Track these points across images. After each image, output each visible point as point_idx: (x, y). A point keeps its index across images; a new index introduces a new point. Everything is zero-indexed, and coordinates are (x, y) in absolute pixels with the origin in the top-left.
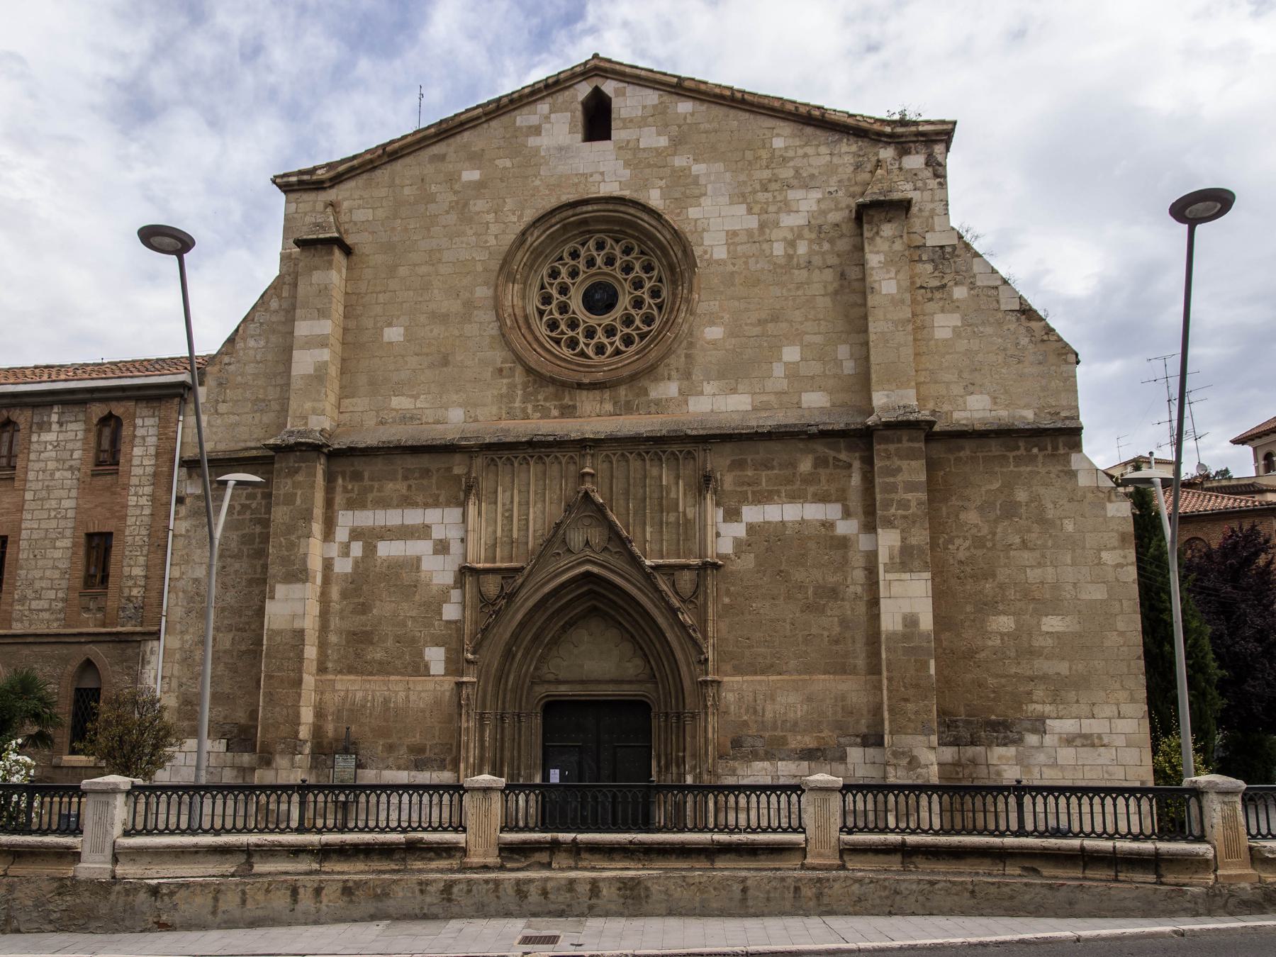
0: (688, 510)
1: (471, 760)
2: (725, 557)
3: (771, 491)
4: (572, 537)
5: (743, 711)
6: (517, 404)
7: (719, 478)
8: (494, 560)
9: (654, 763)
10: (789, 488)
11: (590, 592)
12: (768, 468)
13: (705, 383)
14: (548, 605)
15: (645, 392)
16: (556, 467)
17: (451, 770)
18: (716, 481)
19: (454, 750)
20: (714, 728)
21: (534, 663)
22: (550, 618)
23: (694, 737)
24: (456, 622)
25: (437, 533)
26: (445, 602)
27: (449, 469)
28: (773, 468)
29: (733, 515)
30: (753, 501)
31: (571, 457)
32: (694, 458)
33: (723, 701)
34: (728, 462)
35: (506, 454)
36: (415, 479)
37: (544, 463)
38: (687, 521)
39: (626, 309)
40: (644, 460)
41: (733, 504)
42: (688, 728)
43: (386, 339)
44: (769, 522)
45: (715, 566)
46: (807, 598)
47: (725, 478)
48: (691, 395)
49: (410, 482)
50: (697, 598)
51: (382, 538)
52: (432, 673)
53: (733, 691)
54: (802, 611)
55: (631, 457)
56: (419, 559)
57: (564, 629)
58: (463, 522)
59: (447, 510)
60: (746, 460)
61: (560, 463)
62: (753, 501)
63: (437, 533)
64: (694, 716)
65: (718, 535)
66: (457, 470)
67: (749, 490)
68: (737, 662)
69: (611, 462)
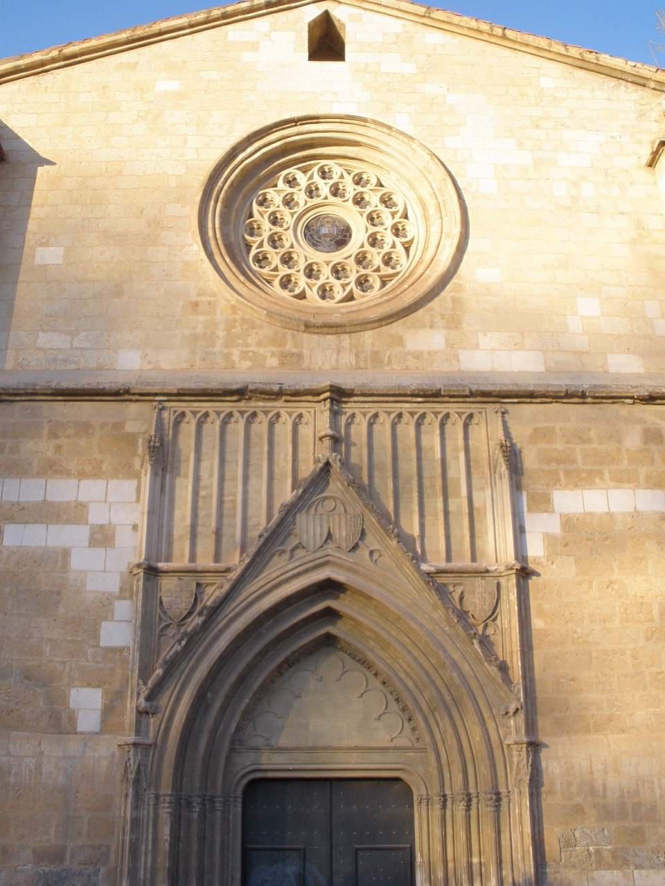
3: (591, 471)
6: (216, 349)
10: (614, 467)
12: (584, 442)
13: (481, 335)
15: (400, 341)
24: (121, 650)
25: (96, 516)
26: (105, 619)
27: (119, 426)
28: (590, 441)
34: (529, 431)
36: (68, 437)
39: (362, 246)
43: (38, 261)
44: (591, 514)
46: (652, 620)
48: (465, 348)
49: (59, 441)
51: (11, 520)
52: (79, 729)
54: (648, 639)
56: (66, 553)
57: (280, 670)
59: (113, 483)
63: (96, 516)
66: (130, 427)
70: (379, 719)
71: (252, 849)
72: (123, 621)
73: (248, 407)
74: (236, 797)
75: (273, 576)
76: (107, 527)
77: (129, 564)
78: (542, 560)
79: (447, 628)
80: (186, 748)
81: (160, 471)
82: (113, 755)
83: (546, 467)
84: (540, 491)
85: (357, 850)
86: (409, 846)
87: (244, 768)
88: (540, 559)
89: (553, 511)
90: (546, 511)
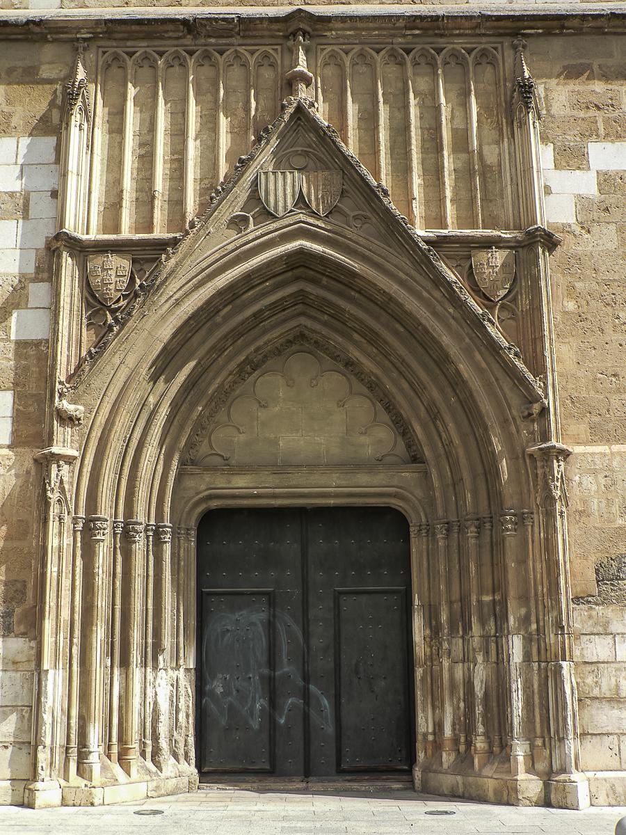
0: (486, 149)
1: (65, 614)
2: (566, 229)
4: (271, 187)
5: (615, 509)
7: (542, 95)
8: (117, 229)
9: (418, 623)
11: (301, 298)
14: (218, 319)
16: (236, 73)
17: (24, 634)
18: (540, 99)
19: (30, 594)
20: (564, 540)
21: (188, 430)
22: (218, 349)
23: (523, 561)
24: (37, 344)
29: (572, 158)
30: (607, 135)
31: (266, 56)
32: (493, 63)
33: (576, 491)
35: (142, 47)
37: (214, 65)
38: (486, 170)
40: (402, 64)
41: (571, 139)
42: (511, 541)
45: (550, 242)
47: (554, 95)
50: (514, 300)
53: (595, 472)
55: (378, 58)
58: (57, 161)
60: (589, 67)
61: (244, 65)
62: (607, 135)
64: (521, 520)
65: (548, 190)
67: (600, 116)
68: (597, 419)
69: (341, 66)
70: (365, 433)
71: (209, 594)
72: (40, 308)
73: (195, 45)
74: (188, 530)
75: (230, 247)
76: (18, 194)
77: (47, 237)
78: (574, 227)
79: (451, 310)
80: (122, 465)
81: (86, 124)
82: (28, 472)
83: (582, 114)
84: (572, 144)
85: (341, 593)
86: (404, 588)
87: (197, 494)
88: (570, 226)
89: (589, 168)
90: (579, 168)
